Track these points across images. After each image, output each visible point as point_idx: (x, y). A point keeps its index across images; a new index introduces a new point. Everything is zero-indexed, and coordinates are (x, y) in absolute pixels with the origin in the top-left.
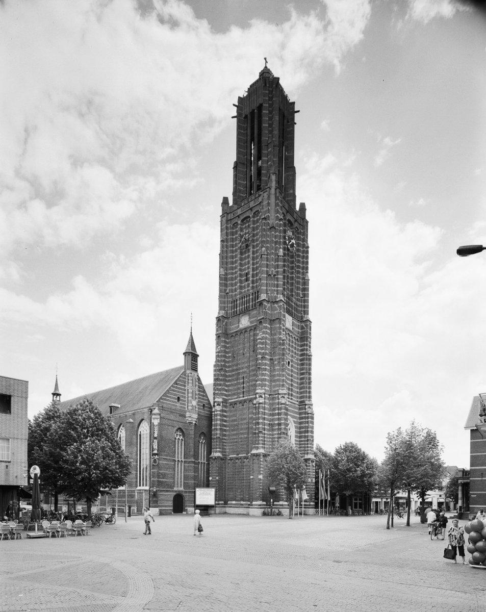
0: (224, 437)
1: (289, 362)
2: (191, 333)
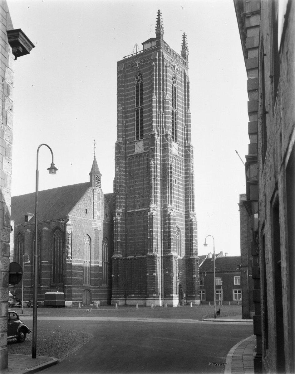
1: (176, 180)
2: (95, 157)
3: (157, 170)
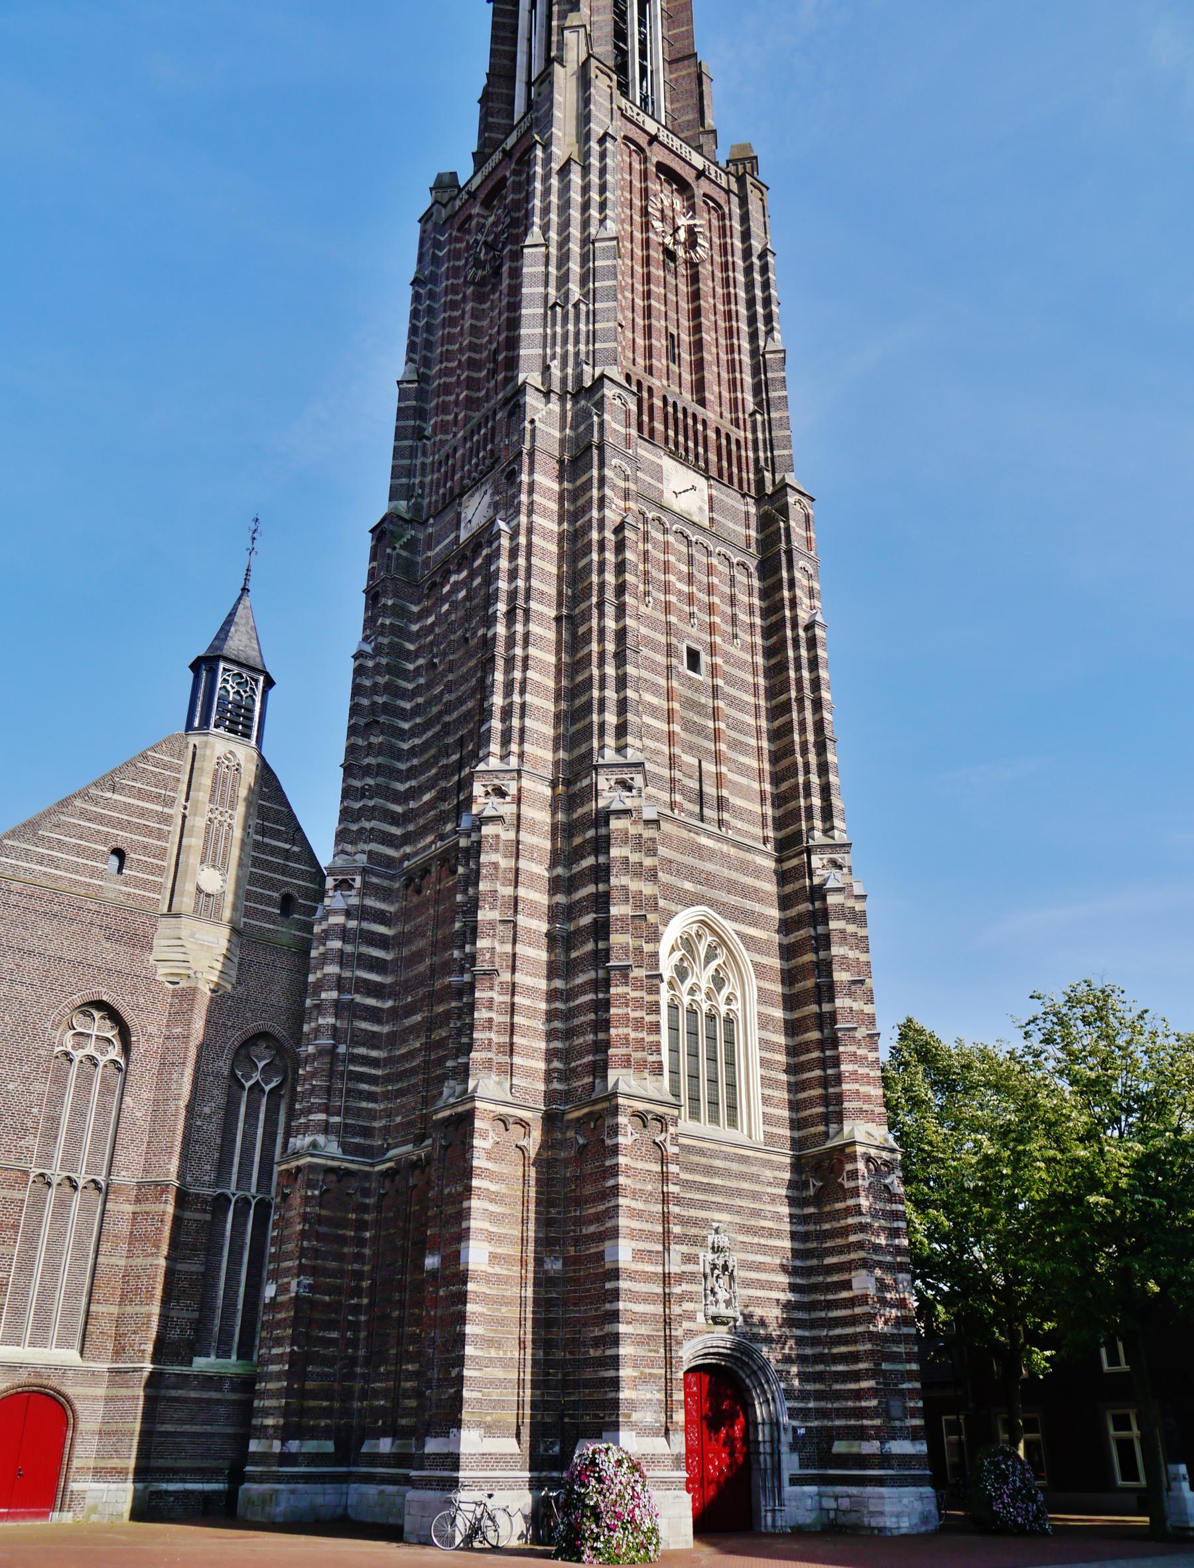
0: (362, 1051)
3: (528, 559)
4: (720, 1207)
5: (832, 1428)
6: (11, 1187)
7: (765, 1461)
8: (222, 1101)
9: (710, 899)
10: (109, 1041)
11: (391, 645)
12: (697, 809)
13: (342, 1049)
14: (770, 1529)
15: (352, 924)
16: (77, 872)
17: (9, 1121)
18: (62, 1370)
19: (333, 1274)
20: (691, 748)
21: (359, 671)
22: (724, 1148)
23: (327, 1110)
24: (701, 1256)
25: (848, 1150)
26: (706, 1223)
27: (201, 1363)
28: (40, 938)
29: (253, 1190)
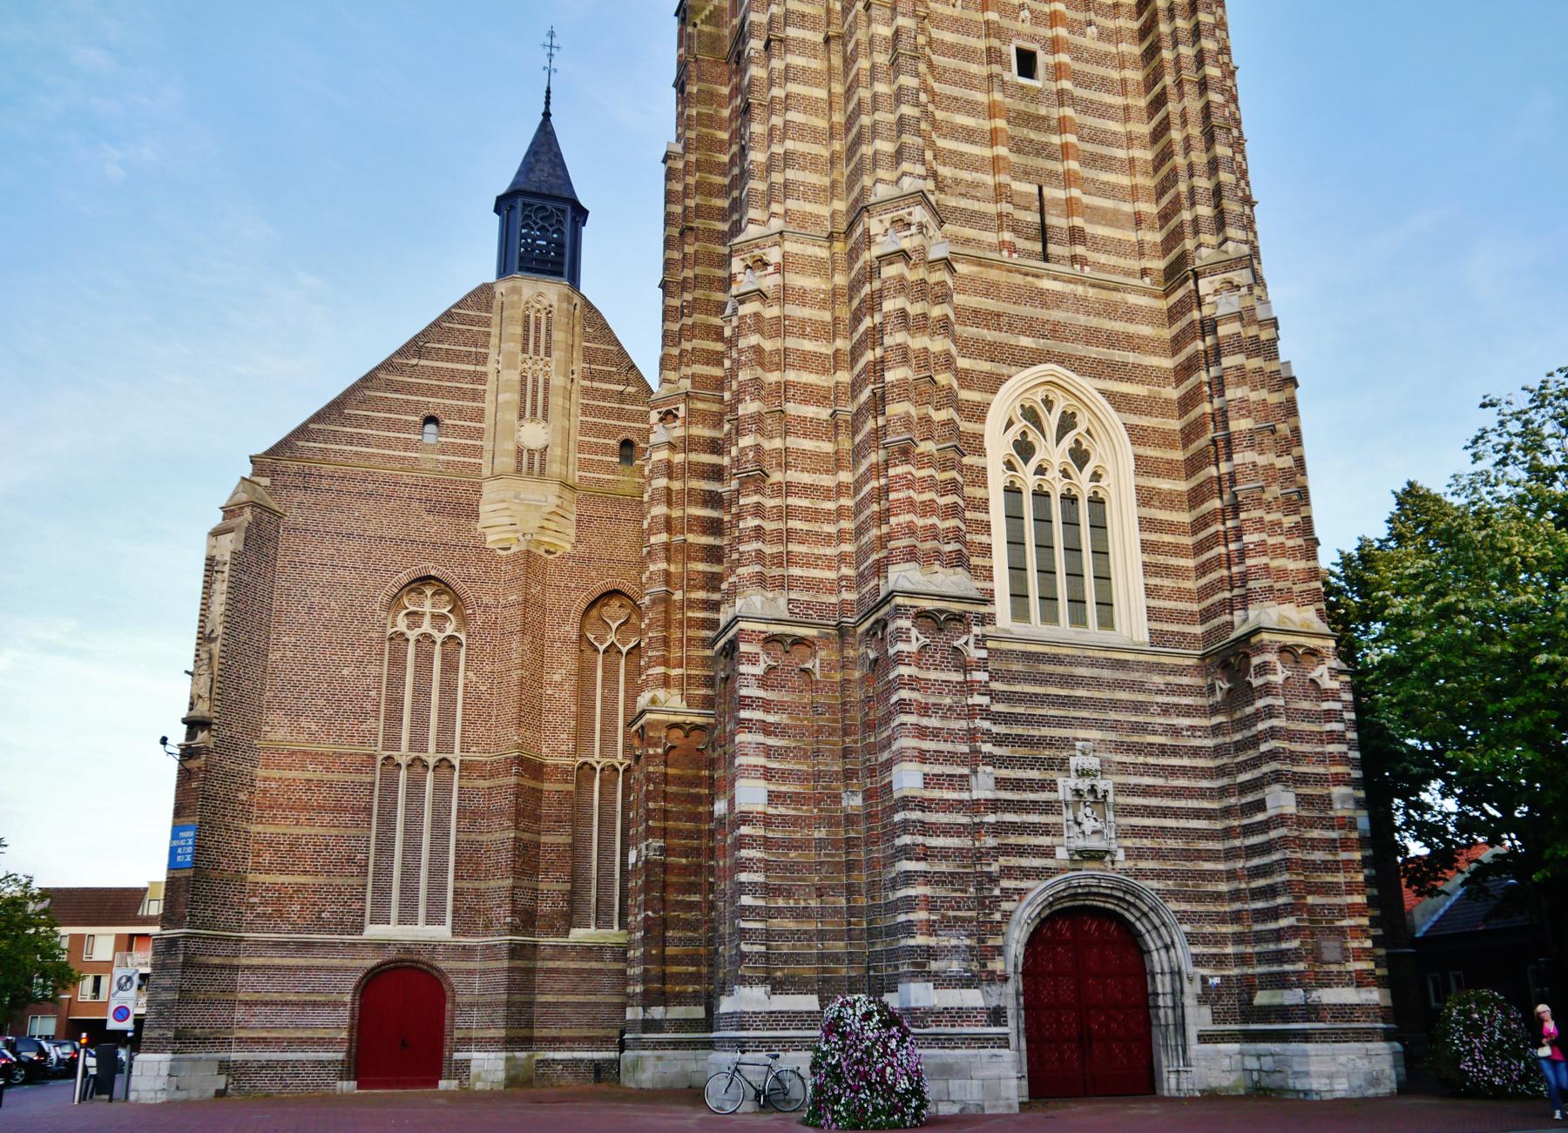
2: (547, 115)
4: (1085, 723)
5: (1253, 976)
6: (359, 771)
7: (1165, 1015)
8: (573, 666)
9: (1059, 355)
10: (444, 617)
11: (699, 138)
12: (1038, 247)
13: (678, 596)
14: (1174, 1093)
15: (678, 458)
16: (390, 447)
17: (348, 706)
18: (432, 947)
19: (689, 835)
20: (1026, 174)
21: (670, 175)
22: (1089, 653)
23: (666, 662)
24: (1060, 781)
25: (1254, 640)
26: (1068, 743)
27: (578, 935)
28: (357, 520)
29: (620, 756)
